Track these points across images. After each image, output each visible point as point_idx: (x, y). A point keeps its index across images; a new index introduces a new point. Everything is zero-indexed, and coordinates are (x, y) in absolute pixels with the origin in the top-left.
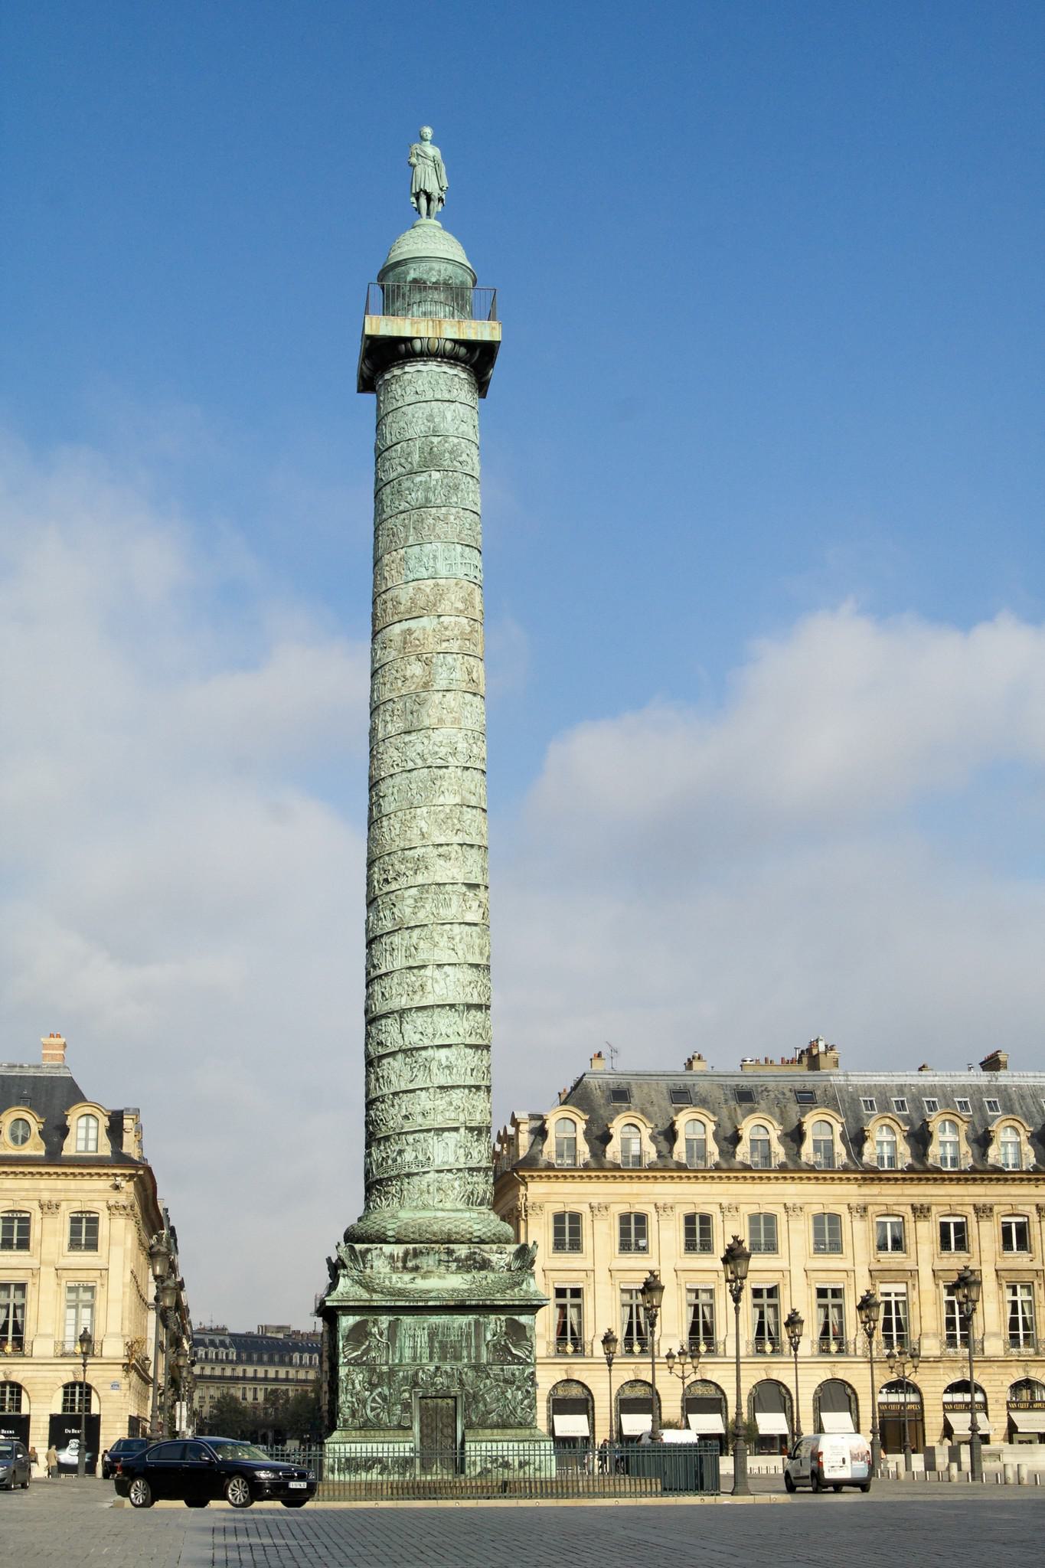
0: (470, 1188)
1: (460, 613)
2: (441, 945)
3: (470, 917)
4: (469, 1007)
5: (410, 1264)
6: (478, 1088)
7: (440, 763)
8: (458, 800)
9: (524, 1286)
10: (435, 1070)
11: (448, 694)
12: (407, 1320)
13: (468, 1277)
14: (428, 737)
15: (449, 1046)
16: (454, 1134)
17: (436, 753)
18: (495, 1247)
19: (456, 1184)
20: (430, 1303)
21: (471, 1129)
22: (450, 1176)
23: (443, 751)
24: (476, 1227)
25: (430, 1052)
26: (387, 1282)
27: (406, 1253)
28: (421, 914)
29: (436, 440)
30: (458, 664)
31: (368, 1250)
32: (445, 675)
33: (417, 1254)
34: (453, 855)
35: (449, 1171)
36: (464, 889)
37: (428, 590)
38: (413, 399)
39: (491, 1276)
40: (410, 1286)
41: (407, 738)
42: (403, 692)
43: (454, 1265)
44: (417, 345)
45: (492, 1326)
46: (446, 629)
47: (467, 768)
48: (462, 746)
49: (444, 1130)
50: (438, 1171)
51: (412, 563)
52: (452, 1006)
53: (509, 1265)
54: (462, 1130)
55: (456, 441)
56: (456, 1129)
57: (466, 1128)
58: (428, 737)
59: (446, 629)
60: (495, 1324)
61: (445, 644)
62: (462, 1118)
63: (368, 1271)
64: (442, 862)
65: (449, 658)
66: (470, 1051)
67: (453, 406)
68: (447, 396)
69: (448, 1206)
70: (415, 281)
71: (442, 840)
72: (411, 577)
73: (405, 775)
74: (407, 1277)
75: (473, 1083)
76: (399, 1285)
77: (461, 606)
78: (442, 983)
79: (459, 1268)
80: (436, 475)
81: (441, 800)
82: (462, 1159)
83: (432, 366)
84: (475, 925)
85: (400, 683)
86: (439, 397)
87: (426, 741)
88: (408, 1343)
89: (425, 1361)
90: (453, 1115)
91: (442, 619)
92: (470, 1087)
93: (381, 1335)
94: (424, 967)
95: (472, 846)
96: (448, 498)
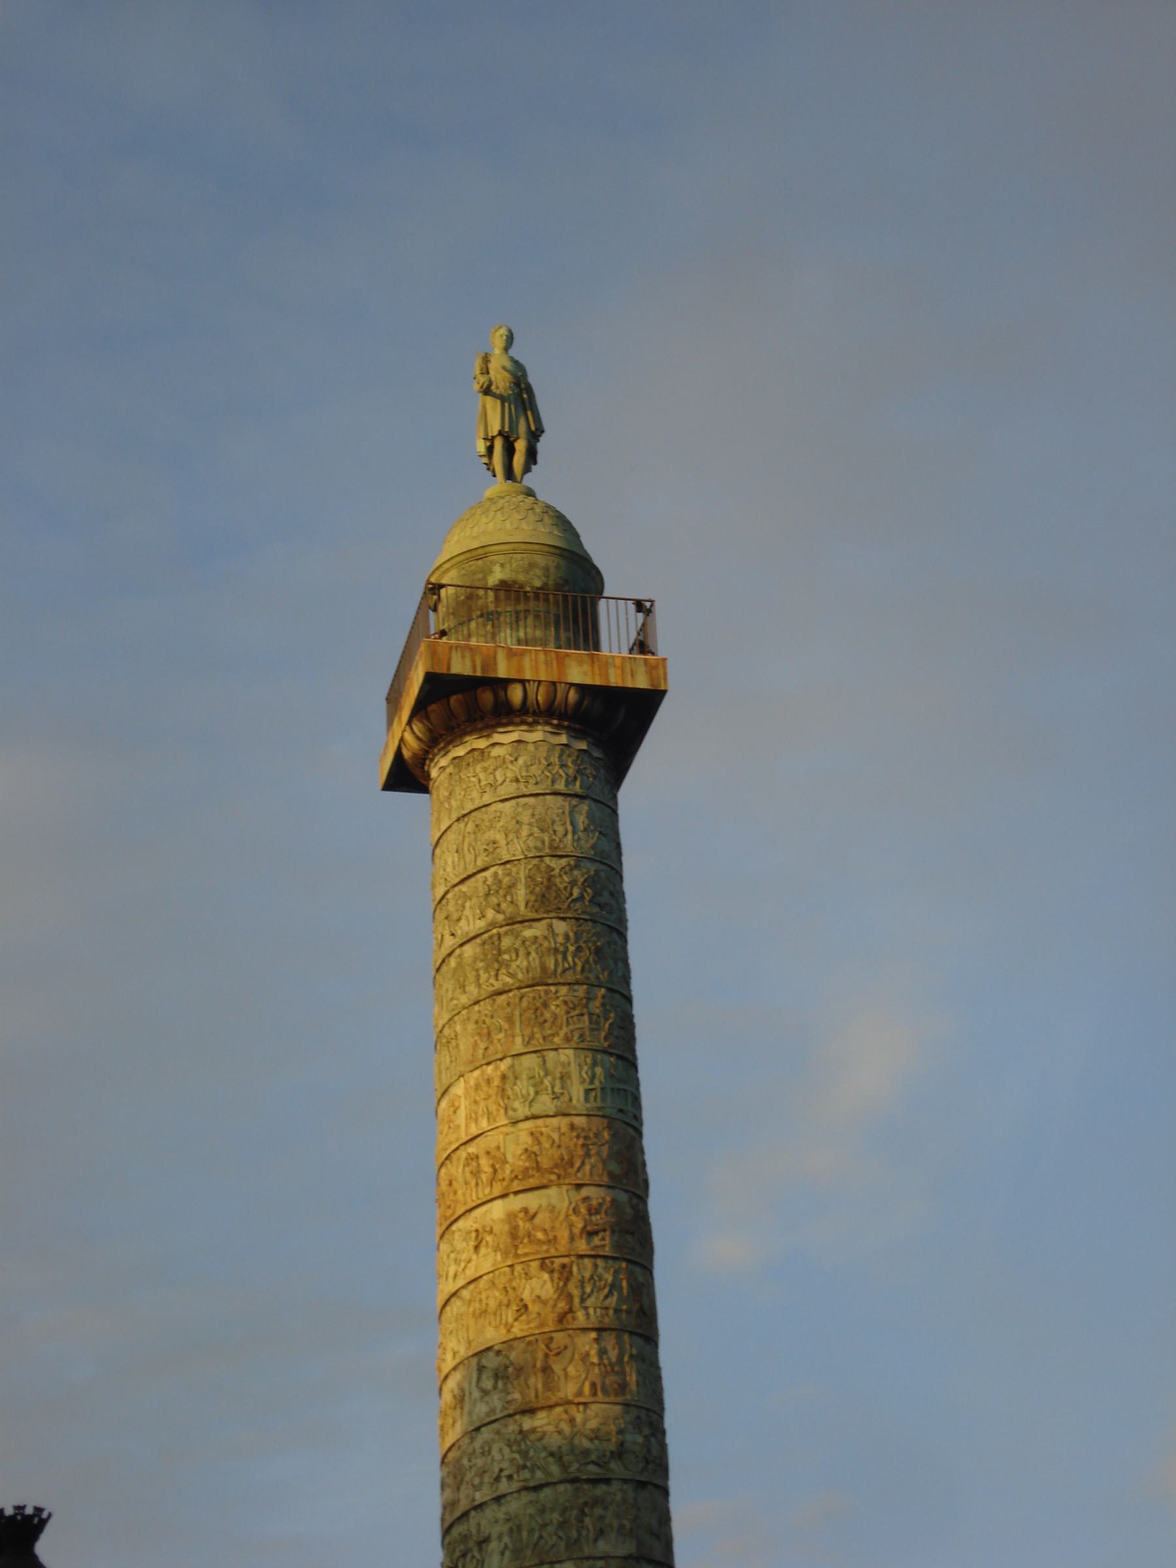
44: (516, 695)
73: (526, 1497)
81: (603, 1546)
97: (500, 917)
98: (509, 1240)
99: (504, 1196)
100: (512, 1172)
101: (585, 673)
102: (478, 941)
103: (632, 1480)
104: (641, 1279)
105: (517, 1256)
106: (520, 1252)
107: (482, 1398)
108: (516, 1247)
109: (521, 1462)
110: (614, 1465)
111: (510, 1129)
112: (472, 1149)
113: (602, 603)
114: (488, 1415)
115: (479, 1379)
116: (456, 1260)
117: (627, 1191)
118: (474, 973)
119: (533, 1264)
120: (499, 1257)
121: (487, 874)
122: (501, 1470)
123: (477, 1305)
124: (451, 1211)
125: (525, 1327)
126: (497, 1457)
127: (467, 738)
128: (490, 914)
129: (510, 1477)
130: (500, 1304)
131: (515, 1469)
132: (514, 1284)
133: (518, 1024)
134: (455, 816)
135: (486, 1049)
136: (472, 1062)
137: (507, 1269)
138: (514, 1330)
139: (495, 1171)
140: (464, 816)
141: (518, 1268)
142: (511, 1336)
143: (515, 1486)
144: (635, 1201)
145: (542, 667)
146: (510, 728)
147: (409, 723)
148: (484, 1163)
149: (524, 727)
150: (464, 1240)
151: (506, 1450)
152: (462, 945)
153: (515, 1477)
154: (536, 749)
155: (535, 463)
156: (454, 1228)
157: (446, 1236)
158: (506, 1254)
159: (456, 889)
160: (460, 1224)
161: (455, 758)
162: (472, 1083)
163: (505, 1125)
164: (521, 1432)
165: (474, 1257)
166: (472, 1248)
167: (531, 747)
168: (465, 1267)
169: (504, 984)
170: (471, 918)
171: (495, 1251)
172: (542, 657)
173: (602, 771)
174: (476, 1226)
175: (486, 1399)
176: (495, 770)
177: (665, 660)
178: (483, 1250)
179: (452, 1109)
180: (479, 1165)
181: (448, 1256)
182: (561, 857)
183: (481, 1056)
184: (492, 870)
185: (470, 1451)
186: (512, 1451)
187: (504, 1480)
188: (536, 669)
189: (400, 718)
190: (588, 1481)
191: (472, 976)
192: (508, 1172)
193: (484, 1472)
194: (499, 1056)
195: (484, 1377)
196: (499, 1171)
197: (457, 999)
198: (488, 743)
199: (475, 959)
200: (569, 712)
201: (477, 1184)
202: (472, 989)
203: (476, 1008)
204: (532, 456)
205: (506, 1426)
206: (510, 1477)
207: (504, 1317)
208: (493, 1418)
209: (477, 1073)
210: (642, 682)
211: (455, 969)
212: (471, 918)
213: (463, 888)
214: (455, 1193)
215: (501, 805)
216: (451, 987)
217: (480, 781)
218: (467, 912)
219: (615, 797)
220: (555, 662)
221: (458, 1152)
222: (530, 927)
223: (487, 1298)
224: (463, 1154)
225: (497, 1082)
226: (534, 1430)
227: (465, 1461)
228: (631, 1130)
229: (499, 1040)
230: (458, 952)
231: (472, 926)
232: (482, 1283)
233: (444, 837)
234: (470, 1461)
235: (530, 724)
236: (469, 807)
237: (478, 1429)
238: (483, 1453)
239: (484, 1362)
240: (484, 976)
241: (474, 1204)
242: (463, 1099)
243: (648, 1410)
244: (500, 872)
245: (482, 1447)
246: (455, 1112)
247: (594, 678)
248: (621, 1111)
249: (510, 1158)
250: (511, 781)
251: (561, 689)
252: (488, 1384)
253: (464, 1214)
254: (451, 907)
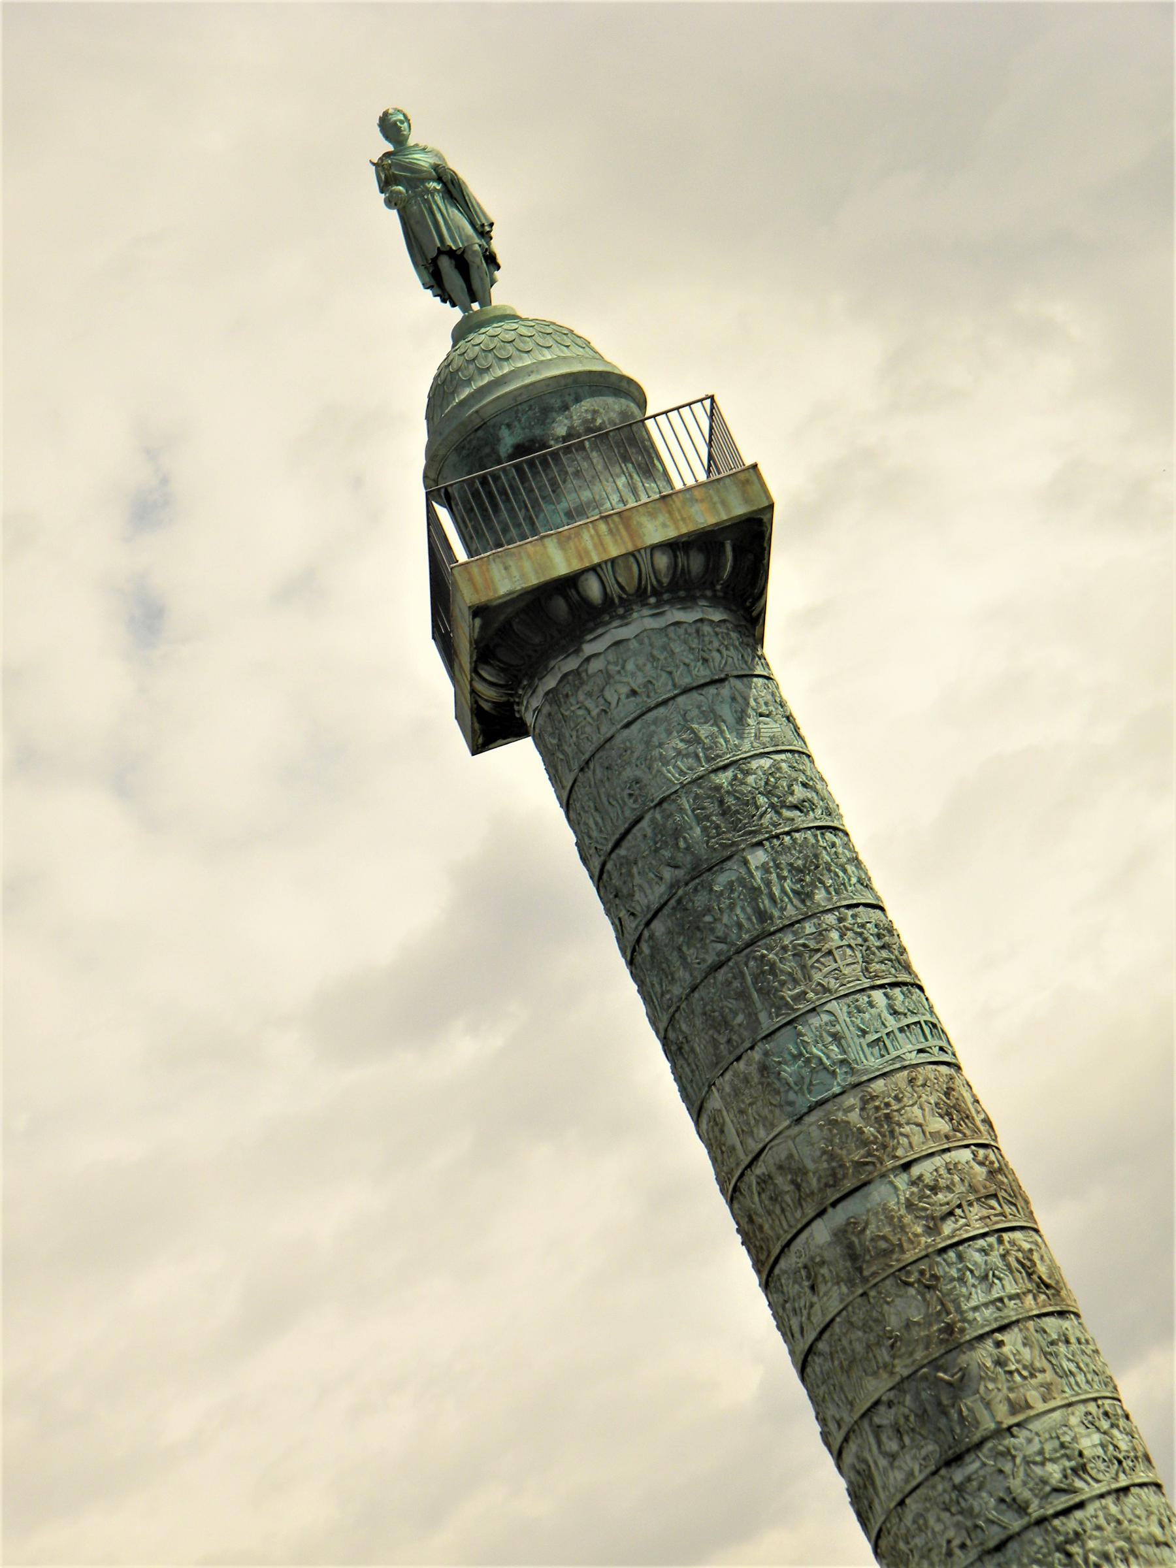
23: (1054, 1472)
30: (995, 1258)
38: (630, 707)
41: (958, 1476)
42: (902, 1370)
44: (593, 589)
47: (1125, 1490)
48: (1089, 1443)
51: (789, 1071)
55: (766, 763)
59: (935, 1189)
61: (948, 1228)
68: (702, 674)
70: (520, 450)
72: (803, 1101)
77: (941, 1125)
80: (758, 858)
83: (643, 621)
85: (884, 1355)
86: (686, 681)
91: (916, 1171)
96: (804, 896)
97: (680, 873)
98: (849, 1264)
99: (821, 1214)
100: (819, 1180)
101: (664, 525)
102: (665, 911)
103: (1109, 1493)
104: (1026, 1246)
105: (865, 1280)
106: (866, 1273)
107: (891, 1465)
108: (860, 1270)
109: (969, 1524)
111: (796, 1130)
112: (760, 1169)
113: (650, 424)
114: (907, 1481)
115: (879, 1443)
116: (794, 1310)
117: (967, 1146)
118: (675, 953)
119: (888, 1282)
120: (844, 1289)
121: (645, 823)
122: (949, 1542)
123: (842, 1356)
124: (765, 1254)
125: (908, 1361)
126: (938, 1528)
127: (552, 663)
128: (668, 874)
129: (963, 1546)
130: (869, 1347)
131: (964, 1533)
132: (875, 1314)
133: (755, 995)
134: (576, 766)
135: (729, 1041)
136: (717, 1064)
137: (859, 1300)
138: (897, 1369)
139: (798, 1187)
140: (587, 762)
141: (873, 1293)
142: (897, 1378)
143: (973, 1554)
144: (981, 1152)
145: (608, 540)
146: (600, 631)
147: (475, 671)
148: (782, 1182)
149: (616, 623)
150: (795, 1282)
151: (945, 1516)
152: (648, 924)
153: (968, 1542)
154: (641, 643)
155: (498, 267)
156: (777, 1271)
157: (772, 1285)
158: (851, 1283)
159: (614, 856)
160: (783, 1264)
161: (547, 694)
162: (727, 1089)
163: (789, 1127)
164: (955, 1487)
165: (815, 1299)
166: (808, 1291)
167: (634, 644)
168: (809, 1315)
169: (719, 954)
170: (646, 886)
171: (838, 1283)
172: (602, 527)
173: (734, 635)
174: (803, 1260)
175: (896, 1463)
176: (602, 690)
177: (755, 466)
178: (822, 1289)
179: (717, 1129)
180: (775, 1185)
181: (784, 1308)
182: (725, 768)
183: (725, 1053)
184: (648, 817)
185: (903, 1531)
186: (953, 1514)
187: (958, 1552)
188: (600, 545)
189: (461, 666)
190: (1057, 1515)
191: (674, 957)
192: (814, 1182)
193: (930, 1550)
194: (747, 1044)
195: (884, 1438)
196: (804, 1185)
197: (668, 992)
198: (580, 660)
199: (670, 932)
200: (666, 581)
201: (783, 1211)
202: (681, 973)
203: (696, 995)
204: (491, 260)
205: (934, 1487)
206: (963, 1546)
207: (880, 1360)
208: (914, 1483)
209: (728, 1076)
210: (739, 509)
211: (652, 956)
212: (646, 886)
213: (622, 851)
214: (761, 1228)
215: (626, 732)
216: (655, 981)
217: (589, 712)
218: (637, 880)
219: (737, 1223)
220: (621, 527)
221: (745, 1178)
222: (722, 871)
223: (851, 1342)
224: (752, 1178)
225: (756, 1078)
226: (969, 1479)
227: (902, 1546)
228: (944, 1069)
229: (740, 1025)
230: (646, 934)
231: (651, 897)
232: (836, 1328)
233: (574, 796)
234: (908, 1543)
235: (622, 617)
236: (589, 748)
237: (902, 1503)
238: (920, 1530)
239: (877, 1420)
240: (691, 953)
241: (789, 1237)
242: (725, 1113)
243: (1095, 1399)
244: (658, 816)
245: (914, 1522)
246: (722, 1131)
247: (677, 528)
248: (921, 1051)
249: (810, 1166)
250: (628, 697)
251: (645, 559)
252: (893, 1446)
253: (782, 1251)
254: (616, 881)
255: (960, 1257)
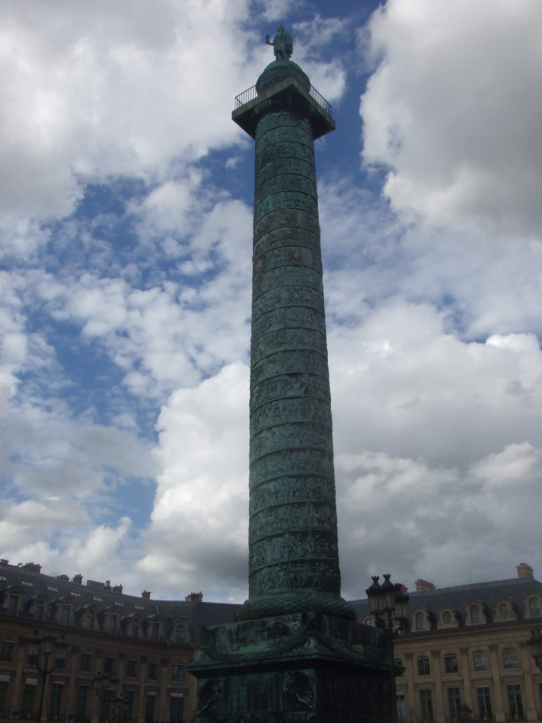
0: (292, 575)
1: (283, 226)
2: (269, 415)
3: (290, 394)
4: (291, 451)
5: (241, 636)
6: (301, 504)
7: (270, 308)
8: (282, 326)
9: (306, 646)
10: (267, 497)
11: (275, 271)
12: (235, 679)
13: (271, 642)
14: (264, 298)
15: (276, 479)
16: (281, 539)
17: (268, 305)
18: (291, 617)
19: (282, 574)
20: (242, 664)
21: (294, 534)
22: (277, 569)
24: (286, 603)
25: (265, 486)
26: (224, 652)
27: (238, 628)
28: (260, 401)
29: (268, 149)
31: (217, 629)
32: (273, 261)
33: (244, 628)
34: (277, 359)
35: (276, 565)
36: (286, 377)
37: (265, 222)
39: (286, 638)
40: (236, 652)
43: (266, 634)
44: (256, 110)
45: (286, 680)
46: (274, 237)
47: (289, 307)
49: (272, 537)
50: (269, 567)
52: (277, 452)
53: (299, 629)
54: (287, 536)
56: (282, 535)
57: (290, 533)
58: (264, 298)
59: (274, 237)
60: (287, 678)
61: (273, 245)
62: (285, 526)
63: (217, 644)
64: (271, 365)
65: (276, 252)
66: (293, 480)
67: (278, 129)
68: (276, 126)
69: (276, 590)
71: (271, 352)
74: (235, 646)
75: (295, 501)
76: (230, 653)
77: (284, 222)
78: (271, 439)
79: (269, 636)
82: (286, 555)
83: (268, 117)
84: (298, 398)
86: (271, 128)
87: (263, 300)
88: (235, 697)
89: (245, 710)
90: (279, 526)
92: (292, 504)
93: (219, 691)
94: (261, 432)
95: (293, 351)
110: (277, 305)
255: (273, 252)
